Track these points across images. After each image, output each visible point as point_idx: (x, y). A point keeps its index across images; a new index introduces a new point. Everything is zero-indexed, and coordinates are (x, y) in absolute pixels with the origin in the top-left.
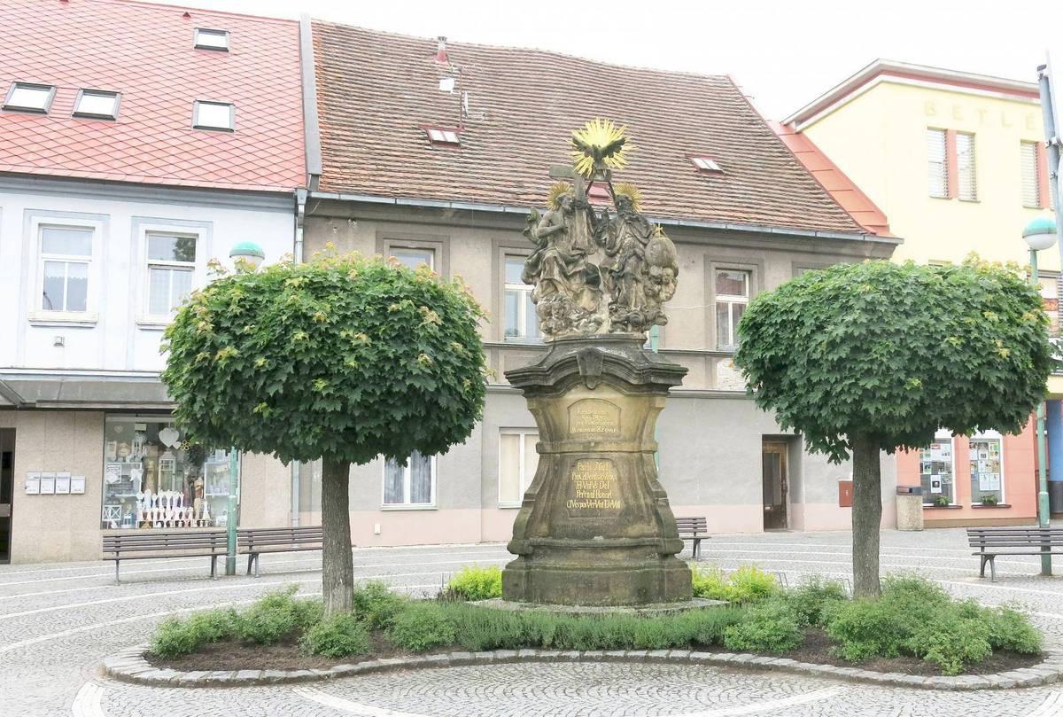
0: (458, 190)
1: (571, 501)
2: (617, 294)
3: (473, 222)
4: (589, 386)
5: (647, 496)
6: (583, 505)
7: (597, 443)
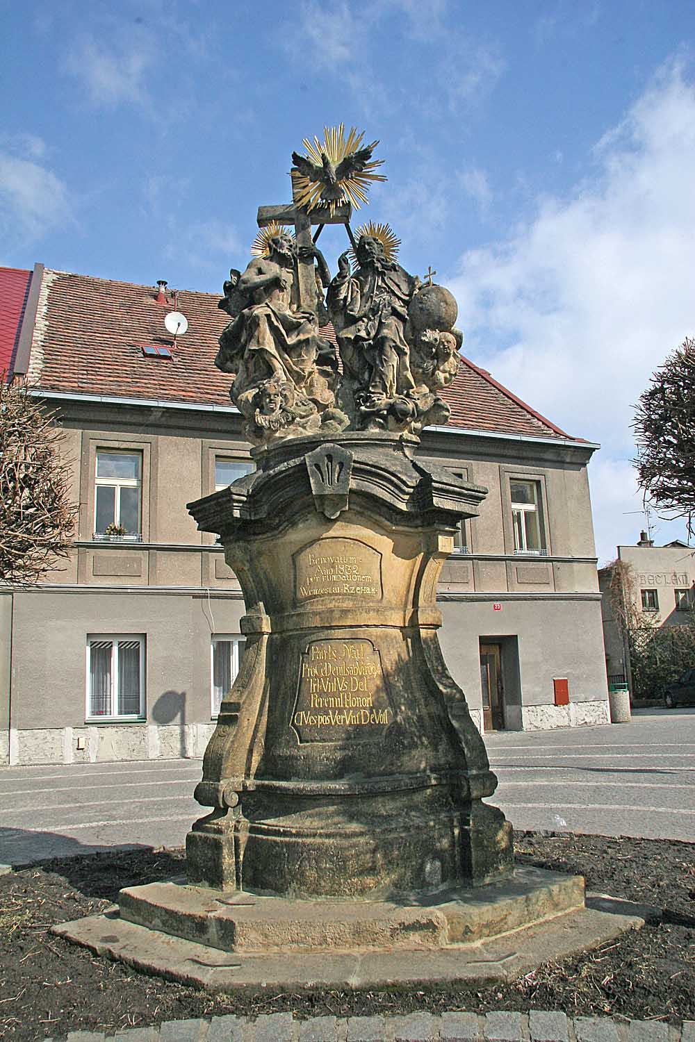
0: (167, 392)
1: (303, 713)
2: (366, 376)
3: (182, 423)
4: (327, 514)
5: (431, 700)
6: (322, 719)
7: (345, 612)
